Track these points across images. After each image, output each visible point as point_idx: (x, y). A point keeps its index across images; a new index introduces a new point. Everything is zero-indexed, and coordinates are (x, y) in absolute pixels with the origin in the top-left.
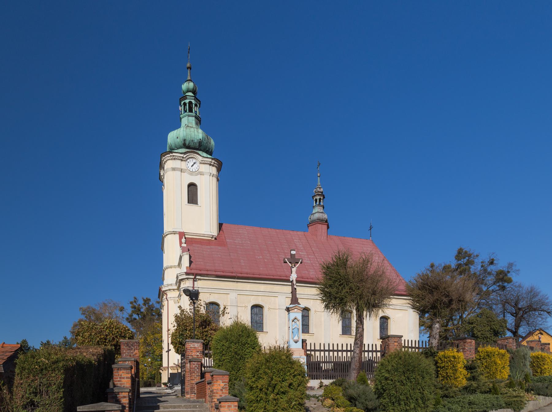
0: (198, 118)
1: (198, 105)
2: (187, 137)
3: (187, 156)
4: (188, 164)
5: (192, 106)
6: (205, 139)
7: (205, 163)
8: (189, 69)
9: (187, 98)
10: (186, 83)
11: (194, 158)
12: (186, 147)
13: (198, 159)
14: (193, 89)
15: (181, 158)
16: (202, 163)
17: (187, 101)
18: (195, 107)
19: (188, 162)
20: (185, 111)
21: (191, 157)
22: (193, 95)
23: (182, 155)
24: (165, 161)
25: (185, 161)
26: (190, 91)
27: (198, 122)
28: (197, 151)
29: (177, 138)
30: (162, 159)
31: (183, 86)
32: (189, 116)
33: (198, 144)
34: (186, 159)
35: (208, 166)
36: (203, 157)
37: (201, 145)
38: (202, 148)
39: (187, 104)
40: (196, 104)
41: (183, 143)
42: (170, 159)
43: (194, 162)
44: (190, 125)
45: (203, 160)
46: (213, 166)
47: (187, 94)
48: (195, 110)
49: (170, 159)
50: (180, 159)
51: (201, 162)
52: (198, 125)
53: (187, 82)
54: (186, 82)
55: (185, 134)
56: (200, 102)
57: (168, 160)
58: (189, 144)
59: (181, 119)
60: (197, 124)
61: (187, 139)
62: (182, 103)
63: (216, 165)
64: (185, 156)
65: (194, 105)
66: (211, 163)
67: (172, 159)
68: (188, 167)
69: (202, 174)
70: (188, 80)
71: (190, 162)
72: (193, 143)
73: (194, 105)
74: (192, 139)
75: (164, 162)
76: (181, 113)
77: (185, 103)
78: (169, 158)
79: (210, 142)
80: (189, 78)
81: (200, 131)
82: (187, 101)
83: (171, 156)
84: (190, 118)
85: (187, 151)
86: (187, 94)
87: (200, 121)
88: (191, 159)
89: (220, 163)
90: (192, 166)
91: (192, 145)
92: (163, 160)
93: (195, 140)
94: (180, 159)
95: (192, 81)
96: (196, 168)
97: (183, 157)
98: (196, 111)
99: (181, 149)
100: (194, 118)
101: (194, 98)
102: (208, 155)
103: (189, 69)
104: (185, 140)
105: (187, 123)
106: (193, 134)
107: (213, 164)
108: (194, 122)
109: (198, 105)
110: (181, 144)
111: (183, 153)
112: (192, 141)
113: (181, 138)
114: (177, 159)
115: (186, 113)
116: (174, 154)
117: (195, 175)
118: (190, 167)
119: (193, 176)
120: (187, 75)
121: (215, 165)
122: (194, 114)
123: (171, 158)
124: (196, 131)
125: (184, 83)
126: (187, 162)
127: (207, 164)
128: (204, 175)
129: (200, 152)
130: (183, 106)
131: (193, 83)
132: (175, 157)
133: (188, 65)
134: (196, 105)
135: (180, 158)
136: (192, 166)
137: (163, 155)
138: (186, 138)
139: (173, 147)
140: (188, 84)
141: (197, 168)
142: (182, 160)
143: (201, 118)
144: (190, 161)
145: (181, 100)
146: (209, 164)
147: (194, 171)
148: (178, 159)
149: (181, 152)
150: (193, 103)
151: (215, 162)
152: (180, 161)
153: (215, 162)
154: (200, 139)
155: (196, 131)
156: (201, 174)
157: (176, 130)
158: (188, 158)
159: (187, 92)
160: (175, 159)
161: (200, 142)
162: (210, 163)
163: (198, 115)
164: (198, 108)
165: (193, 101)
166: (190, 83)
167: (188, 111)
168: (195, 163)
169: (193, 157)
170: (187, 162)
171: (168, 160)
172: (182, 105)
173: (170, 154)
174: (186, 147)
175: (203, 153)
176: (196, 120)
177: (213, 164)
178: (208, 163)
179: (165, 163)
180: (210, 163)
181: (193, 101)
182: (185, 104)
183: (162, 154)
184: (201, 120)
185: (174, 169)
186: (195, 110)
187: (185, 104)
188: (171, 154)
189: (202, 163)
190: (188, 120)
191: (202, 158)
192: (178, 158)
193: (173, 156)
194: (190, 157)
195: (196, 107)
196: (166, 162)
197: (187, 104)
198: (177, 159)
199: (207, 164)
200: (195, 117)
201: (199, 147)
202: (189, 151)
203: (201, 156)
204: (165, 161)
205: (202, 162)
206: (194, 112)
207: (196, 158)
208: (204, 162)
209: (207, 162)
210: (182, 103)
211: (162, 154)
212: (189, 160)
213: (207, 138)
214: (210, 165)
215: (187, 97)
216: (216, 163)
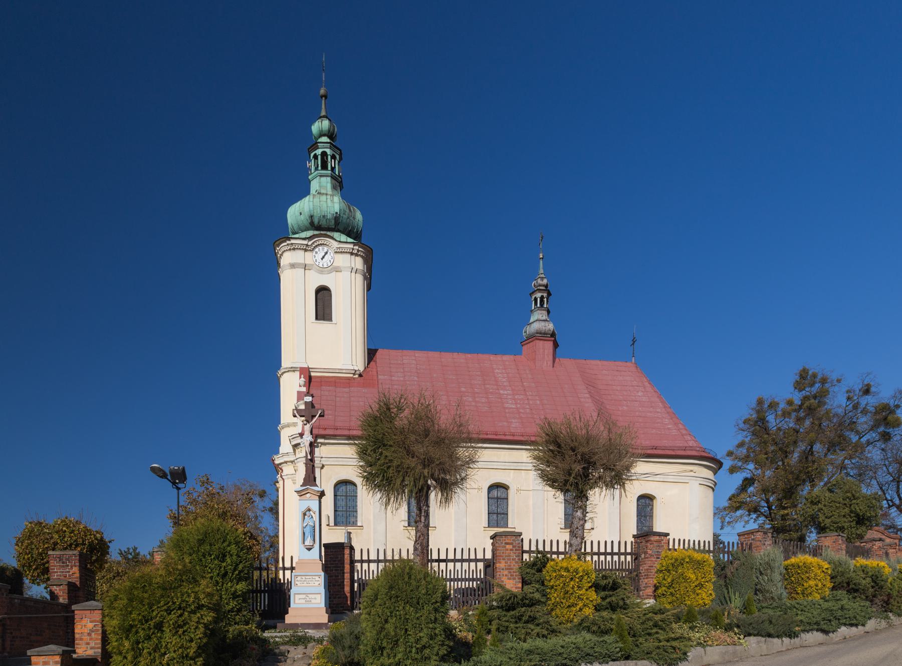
0: (336, 178)
1: (338, 157)
2: (315, 211)
3: (313, 243)
6: (345, 211)
7: (344, 252)
8: (324, 98)
9: (318, 146)
10: (317, 122)
11: (326, 244)
12: (315, 227)
13: (330, 245)
14: (329, 131)
15: (305, 247)
16: (339, 252)
17: (319, 152)
18: (331, 161)
19: (316, 253)
20: (316, 169)
21: (321, 244)
22: (328, 140)
23: (305, 242)
24: (280, 253)
25: (310, 250)
26: (324, 135)
27: (338, 184)
28: (329, 233)
29: (301, 214)
30: (277, 251)
31: (313, 127)
32: (321, 176)
33: (333, 222)
34: (312, 247)
35: (348, 256)
36: (340, 242)
37: (339, 223)
38: (341, 227)
40: (333, 155)
41: (309, 221)
42: (287, 250)
43: (326, 250)
44: (323, 191)
45: (339, 248)
46: (357, 255)
47: (320, 140)
48: (331, 165)
49: (287, 250)
50: (303, 249)
51: (336, 250)
52: (336, 190)
53: (320, 120)
54: (318, 119)
55: (312, 207)
56: (340, 150)
57: (285, 251)
58: (319, 223)
59: (310, 182)
60: (334, 188)
61: (315, 214)
62: (312, 155)
63: (362, 254)
64: (310, 243)
65: (329, 157)
66: (353, 252)
67: (290, 249)
68: (316, 260)
70: (321, 117)
71: (318, 252)
72: (325, 221)
73: (329, 157)
74: (323, 214)
75: (279, 256)
77: (315, 154)
78: (286, 248)
79: (354, 216)
81: (337, 199)
82: (319, 152)
83: (288, 244)
84: (323, 179)
85: (314, 235)
86: (320, 140)
87: (341, 183)
88: (321, 248)
89: (369, 249)
90: (322, 259)
91: (324, 223)
92: (278, 252)
93: (329, 215)
94: (303, 249)
95: (327, 117)
97: (307, 245)
98: (333, 166)
99: (305, 232)
100: (329, 179)
101: (329, 145)
102: (348, 238)
103: (324, 98)
104: (311, 217)
105: (318, 188)
106: (325, 205)
107: (356, 252)
108: (329, 186)
109: (338, 157)
110: (307, 223)
111: (307, 238)
113: (307, 214)
114: (297, 249)
115: (317, 172)
116: (293, 241)
117: (326, 273)
118: (319, 259)
119: (324, 275)
120: (321, 108)
121: (360, 253)
122: (330, 172)
123: (289, 248)
124: (329, 201)
125: (315, 122)
126: (314, 252)
127: (346, 252)
128: (341, 272)
129: (336, 235)
131: (329, 120)
132: (294, 247)
133: (322, 91)
134: (333, 157)
135: (302, 247)
136: (322, 259)
138: (314, 212)
139: (295, 229)
140: (320, 123)
142: (306, 250)
143: (341, 178)
144: (319, 250)
145: (310, 150)
146: (349, 252)
147: (325, 266)
148: (300, 249)
149: (304, 237)
150: (329, 153)
151: (360, 249)
152: (302, 252)
153: (360, 249)
154: (337, 213)
155: (329, 201)
156: (338, 270)
157: (299, 202)
158: (316, 246)
159: (319, 137)
160: (294, 249)
161: (336, 217)
162: (351, 251)
163: (337, 173)
164: (337, 162)
165: (328, 151)
166: (323, 122)
167: (320, 168)
168: (326, 253)
169: (323, 244)
170: (314, 252)
171: (285, 251)
173: (286, 242)
174: (315, 227)
175: (342, 234)
176: (334, 181)
177: (356, 252)
178: (348, 251)
179: (280, 257)
180: (351, 251)
181: (328, 151)
182: (316, 157)
184: (342, 181)
186: (331, 165)
188: (288, 242)
189: (339, 252)
191: (338, 244)
192: (299, 247)
193: (292, 244)
194: (319, 243)
195: (333, 160)
196: (282, 255)
198: (297, 249)
199: (346, 252)
200: (331, 177)
201: (335, 227)
202: (317, 235)
203: (336, 240)
204: (280, 253)
205: (338, 250)
206: (329, 168)
207: (328, 245)
208: (341, 250)
209: (346, 250)
210: (312, 155)
212: (317, 250)
213: (348, 211)
214: (352, 254)
215: (319, 144)
216: (361, 251)
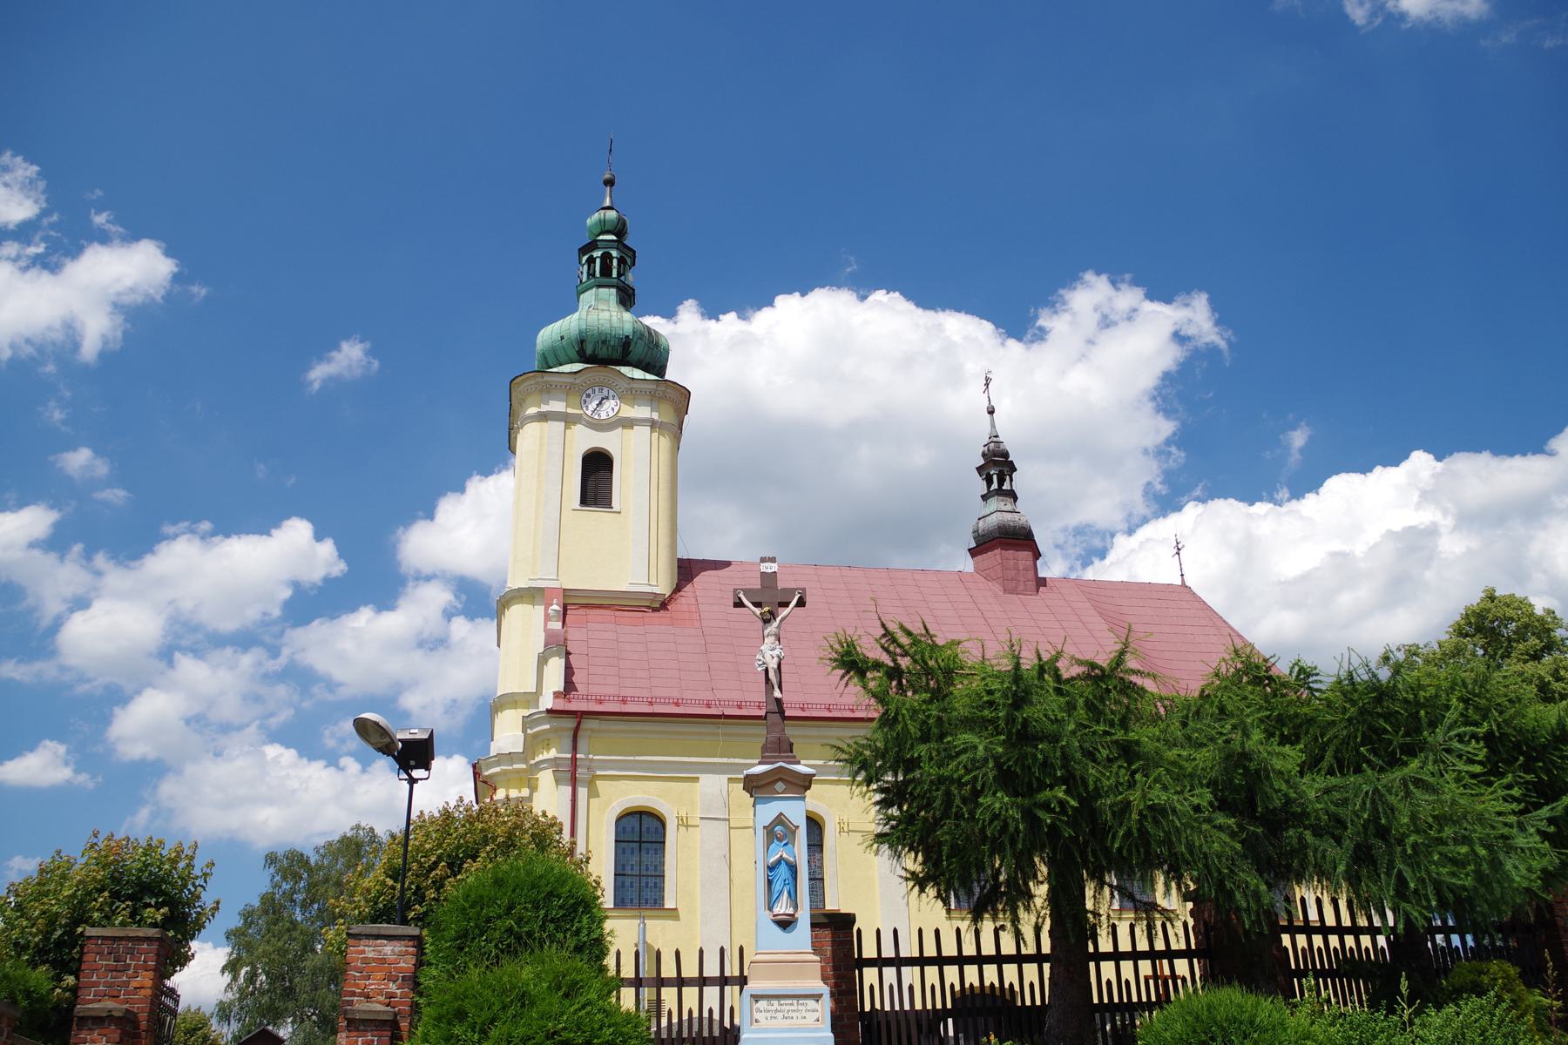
4: (587, 399)
5: (612, 262)
17: (597, 254)
39: (598, 261)
58: (594, 352)
62: (584, 259)
65: (615, 262)
69: (629, 423)
72: (604, 350)
73: (615, 262)
74: (603, 338)
76: (581, 281)
80: (607, 203)
91: (603, 352)
96: (610, 410)
99: (570, 365)
100: (613, 291)
104: (582, 341)
109: (629, 260)
112: (604, 342)
130: (586, 267)
137: (514, 382)
141: (613, 409)
144: (594, 392)
154: (627, 337)
167: (598, 274)
172: (584, 262)
182: (591, 261)
183: (514, 380)
185: (543, 417)
187: (591, 261)
190: (597, 295)
197: (598, 261)
211: (514, 380)
